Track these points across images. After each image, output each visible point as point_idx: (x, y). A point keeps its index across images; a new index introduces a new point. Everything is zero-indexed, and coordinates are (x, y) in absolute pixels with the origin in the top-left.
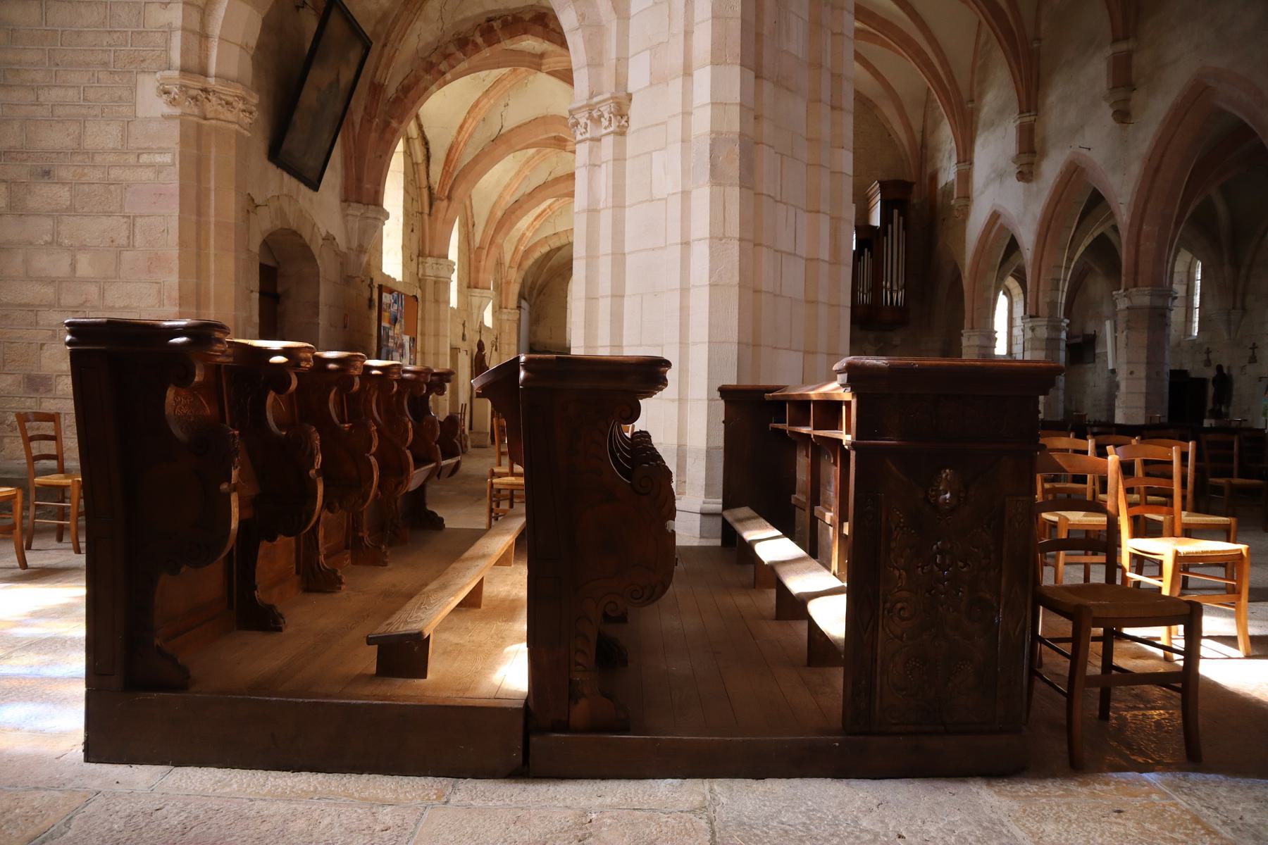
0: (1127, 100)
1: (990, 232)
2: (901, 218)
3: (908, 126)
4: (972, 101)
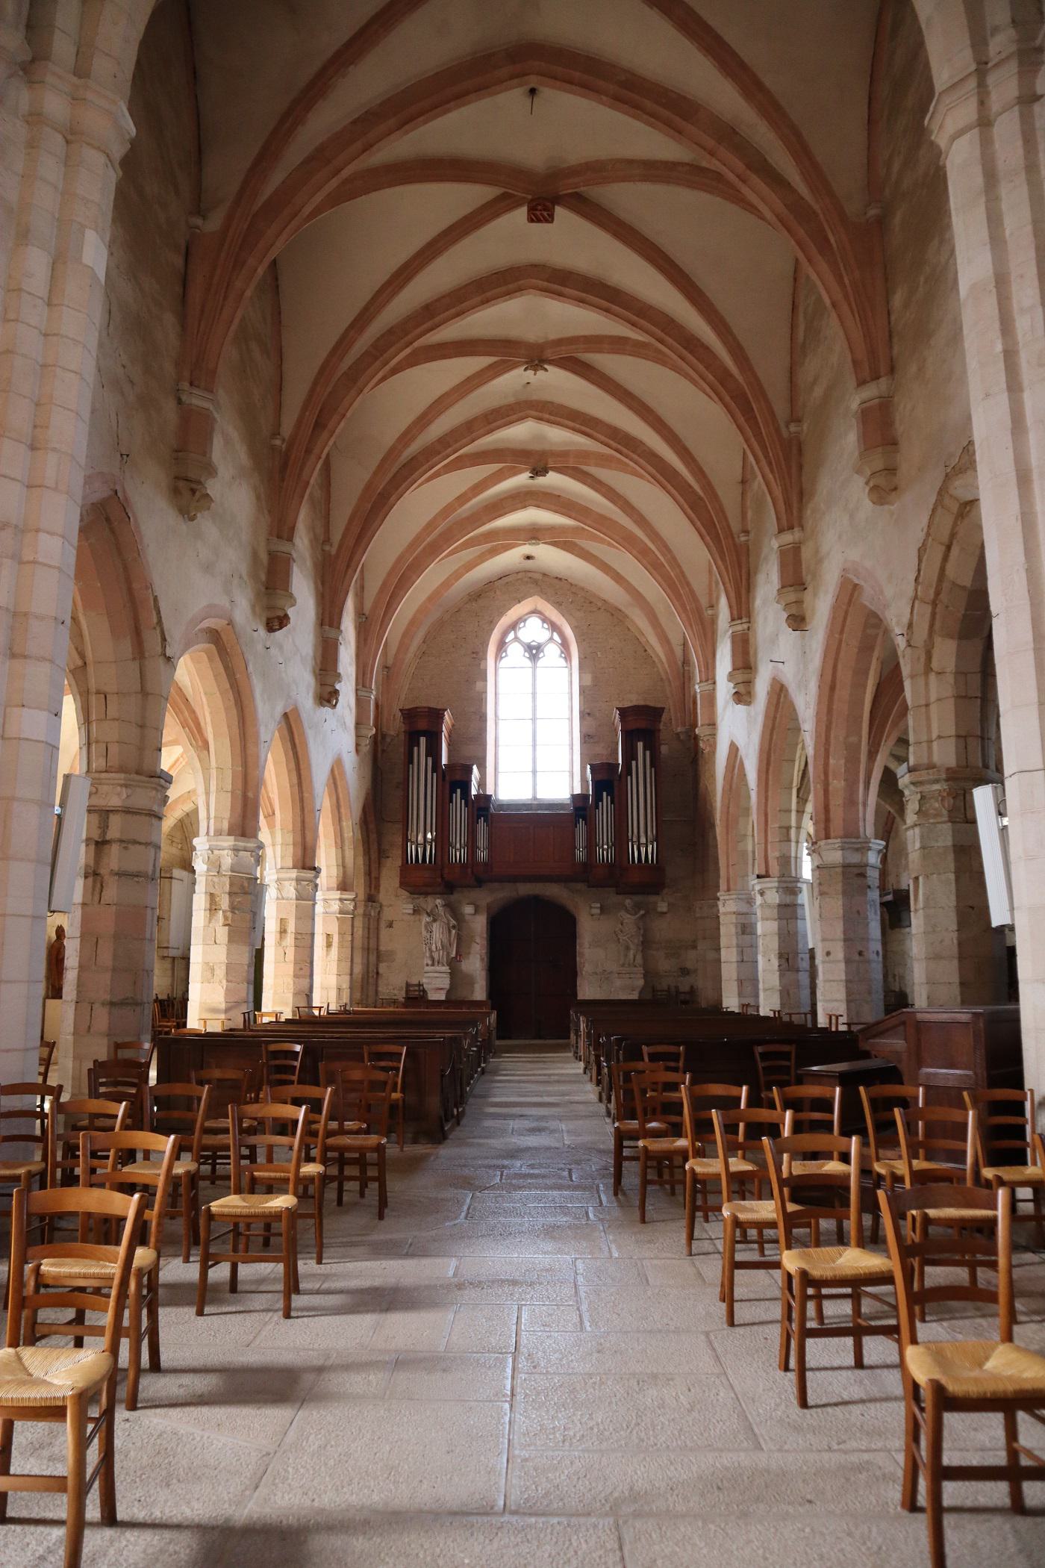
0: (799, 602)
1: (734, 767)
2: (648, 753)
3: (664, 639)
4: (712, 606)
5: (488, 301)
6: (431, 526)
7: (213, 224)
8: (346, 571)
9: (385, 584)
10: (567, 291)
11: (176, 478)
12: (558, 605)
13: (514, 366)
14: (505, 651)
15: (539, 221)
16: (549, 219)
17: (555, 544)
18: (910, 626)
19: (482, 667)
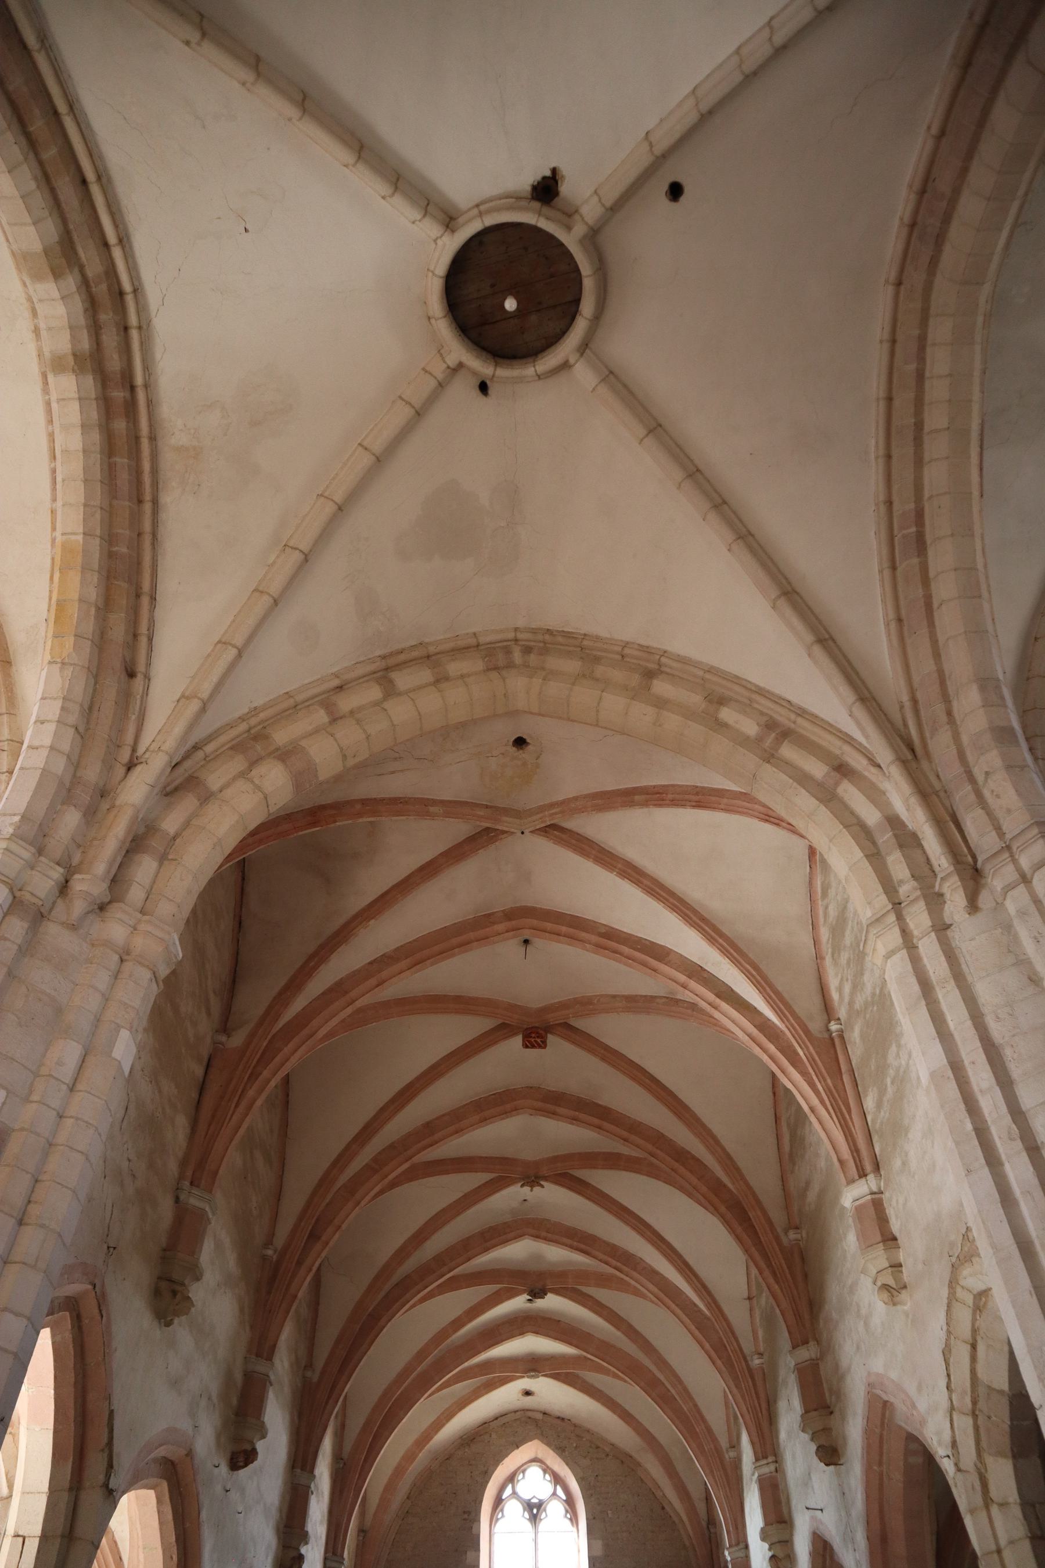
0: (827, 1430)
5: (486, 1119)
6: (421, 1355)
7: (237, 1040)
8: (327, 1403)
9: (368, 1423)
10: (561, 1110)
11: (160, 1278)
12: (560, 1450)
13: (511, 1182)
14: (502, 1510)
15: (533, 1047)
16: (543, 1045)
17: (556, 1377)
18: (954, 1444)
19: (474, 1531)
